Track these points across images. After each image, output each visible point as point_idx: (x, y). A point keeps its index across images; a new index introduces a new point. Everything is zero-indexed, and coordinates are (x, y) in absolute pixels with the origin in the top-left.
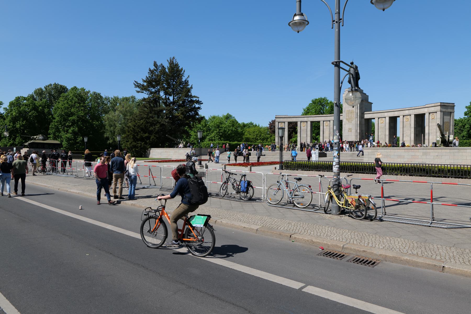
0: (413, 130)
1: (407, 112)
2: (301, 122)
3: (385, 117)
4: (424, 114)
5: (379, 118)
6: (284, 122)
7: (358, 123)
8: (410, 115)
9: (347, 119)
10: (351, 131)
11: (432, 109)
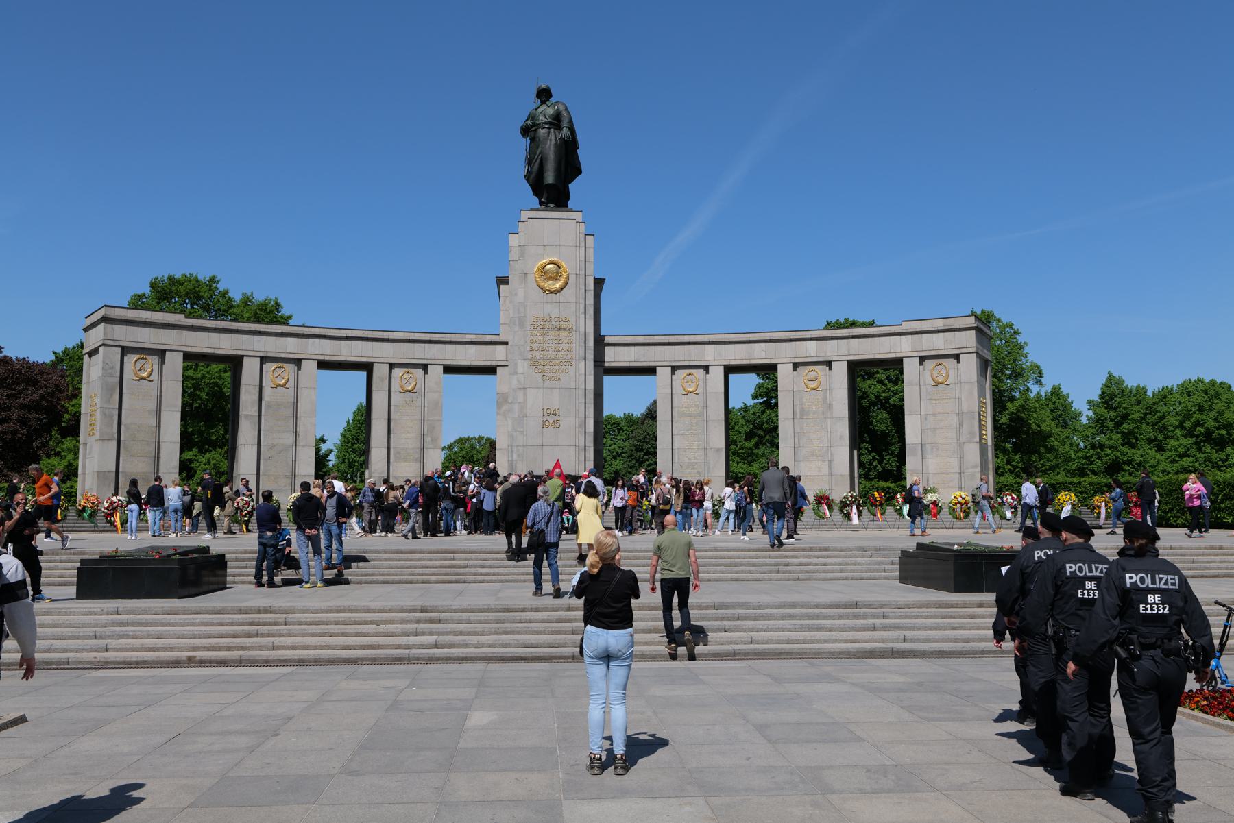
0: (842, 430)
1: (811, 350)
2: (263, 360)
3: (706, 368)
5: (674, 369)
6: (162, 354)
7: (591, 385)
8: (829, 364)
9: (534, 363)
10: (556, 425)
11: (938, 343)
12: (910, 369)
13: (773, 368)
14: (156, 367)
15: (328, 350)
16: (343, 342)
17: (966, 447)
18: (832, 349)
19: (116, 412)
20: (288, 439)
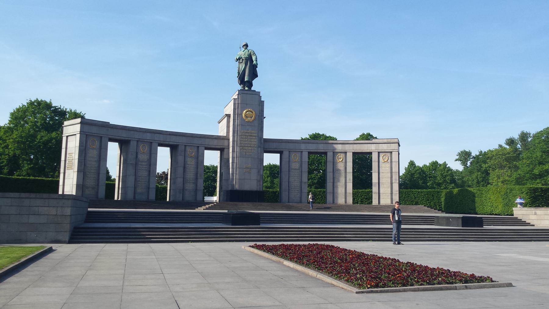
4: (370, 153)
8: (346, 152)
11: (384, 147)
12: (375, 157)
13: (326, 153)
14: (99, 143)
15: (161, 138)
16: (168, 136)
17: (393, 185)
18: (347, 147)
19: (83, 161)
20: (145, 173)
